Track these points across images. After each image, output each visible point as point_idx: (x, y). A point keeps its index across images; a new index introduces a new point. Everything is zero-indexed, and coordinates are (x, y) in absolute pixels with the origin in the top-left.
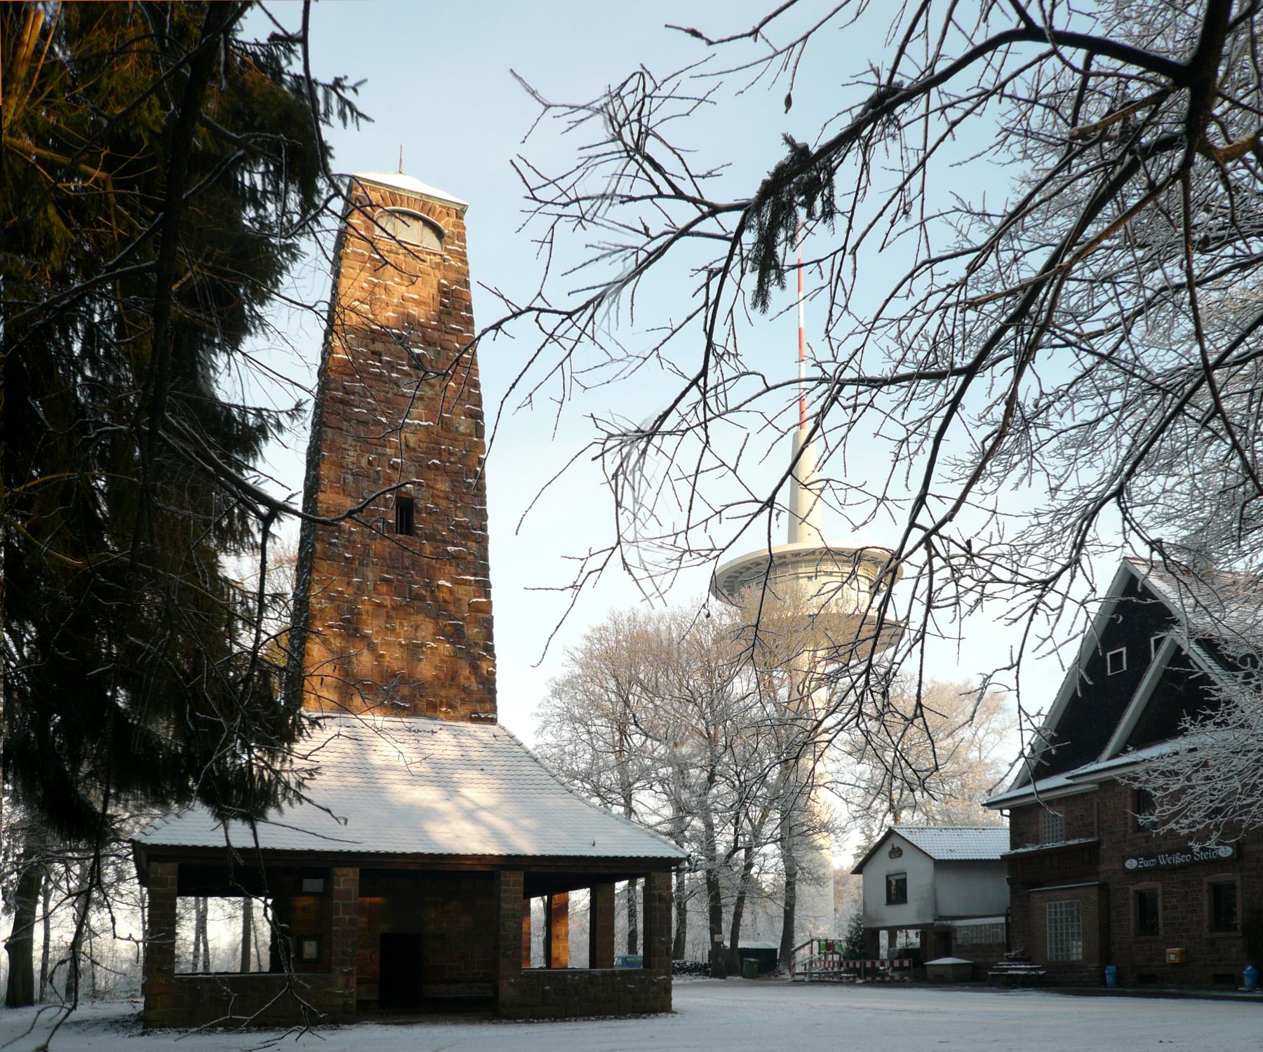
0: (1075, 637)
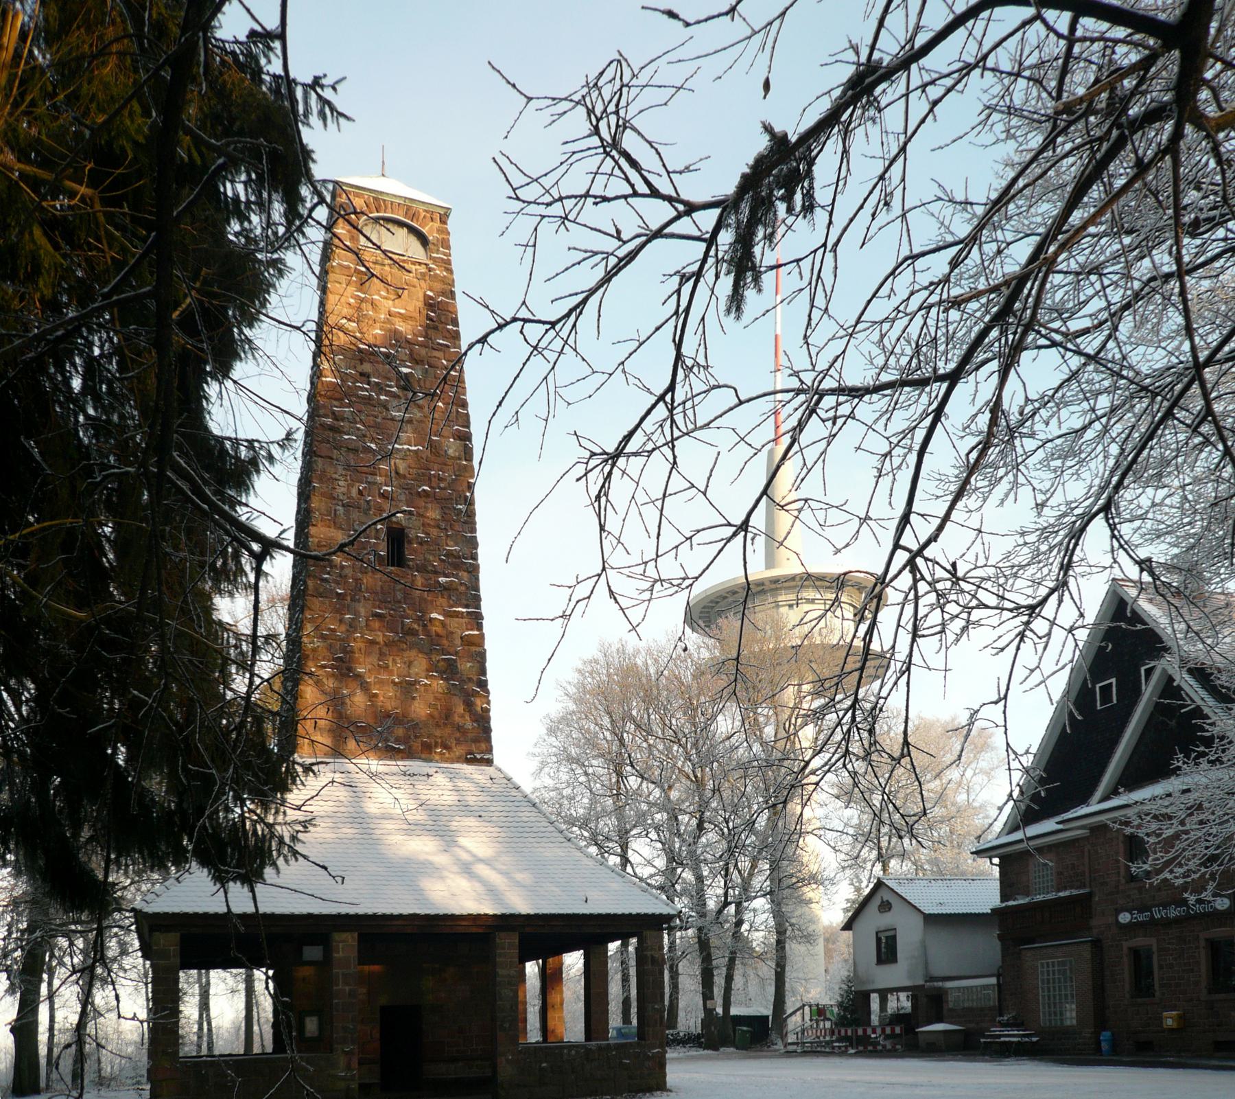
0: (1063, 668)
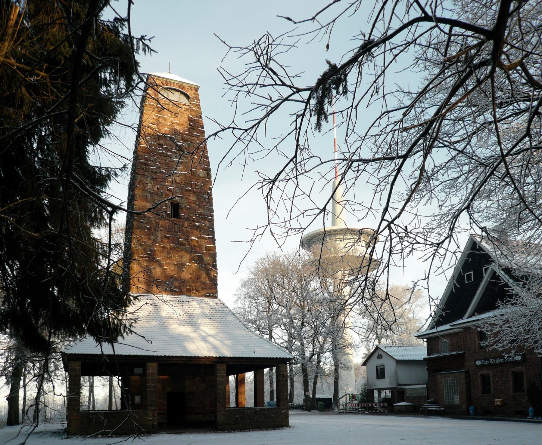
0: (451, 267)
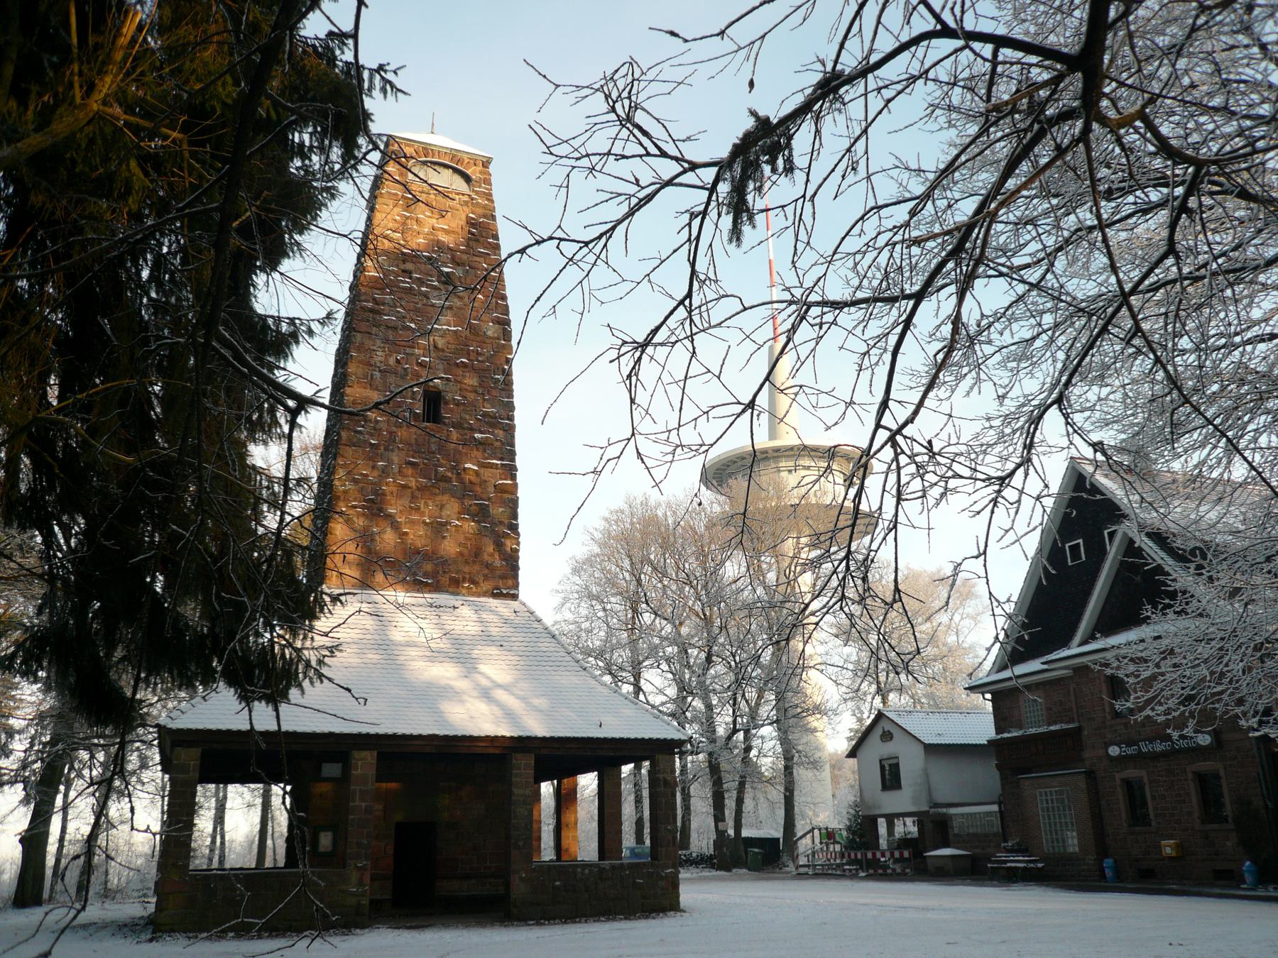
0: (1034, 529)
